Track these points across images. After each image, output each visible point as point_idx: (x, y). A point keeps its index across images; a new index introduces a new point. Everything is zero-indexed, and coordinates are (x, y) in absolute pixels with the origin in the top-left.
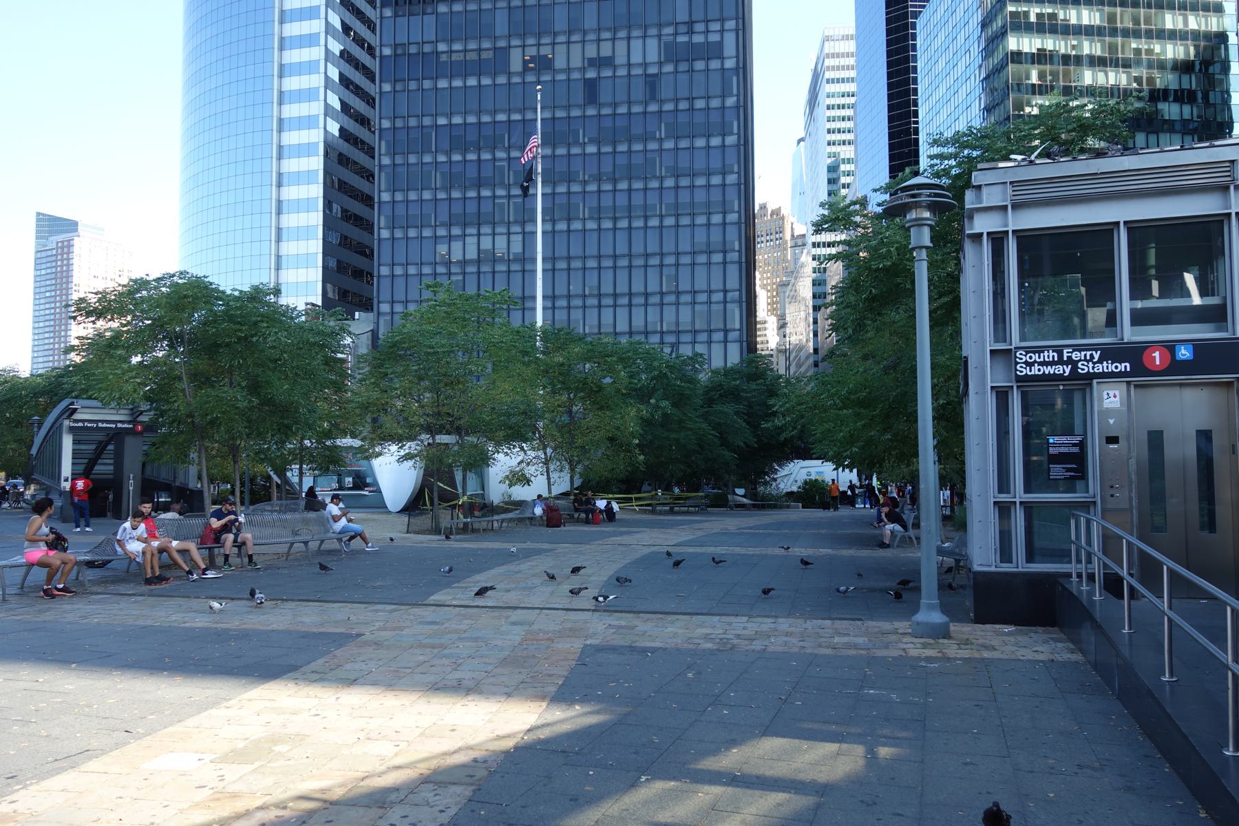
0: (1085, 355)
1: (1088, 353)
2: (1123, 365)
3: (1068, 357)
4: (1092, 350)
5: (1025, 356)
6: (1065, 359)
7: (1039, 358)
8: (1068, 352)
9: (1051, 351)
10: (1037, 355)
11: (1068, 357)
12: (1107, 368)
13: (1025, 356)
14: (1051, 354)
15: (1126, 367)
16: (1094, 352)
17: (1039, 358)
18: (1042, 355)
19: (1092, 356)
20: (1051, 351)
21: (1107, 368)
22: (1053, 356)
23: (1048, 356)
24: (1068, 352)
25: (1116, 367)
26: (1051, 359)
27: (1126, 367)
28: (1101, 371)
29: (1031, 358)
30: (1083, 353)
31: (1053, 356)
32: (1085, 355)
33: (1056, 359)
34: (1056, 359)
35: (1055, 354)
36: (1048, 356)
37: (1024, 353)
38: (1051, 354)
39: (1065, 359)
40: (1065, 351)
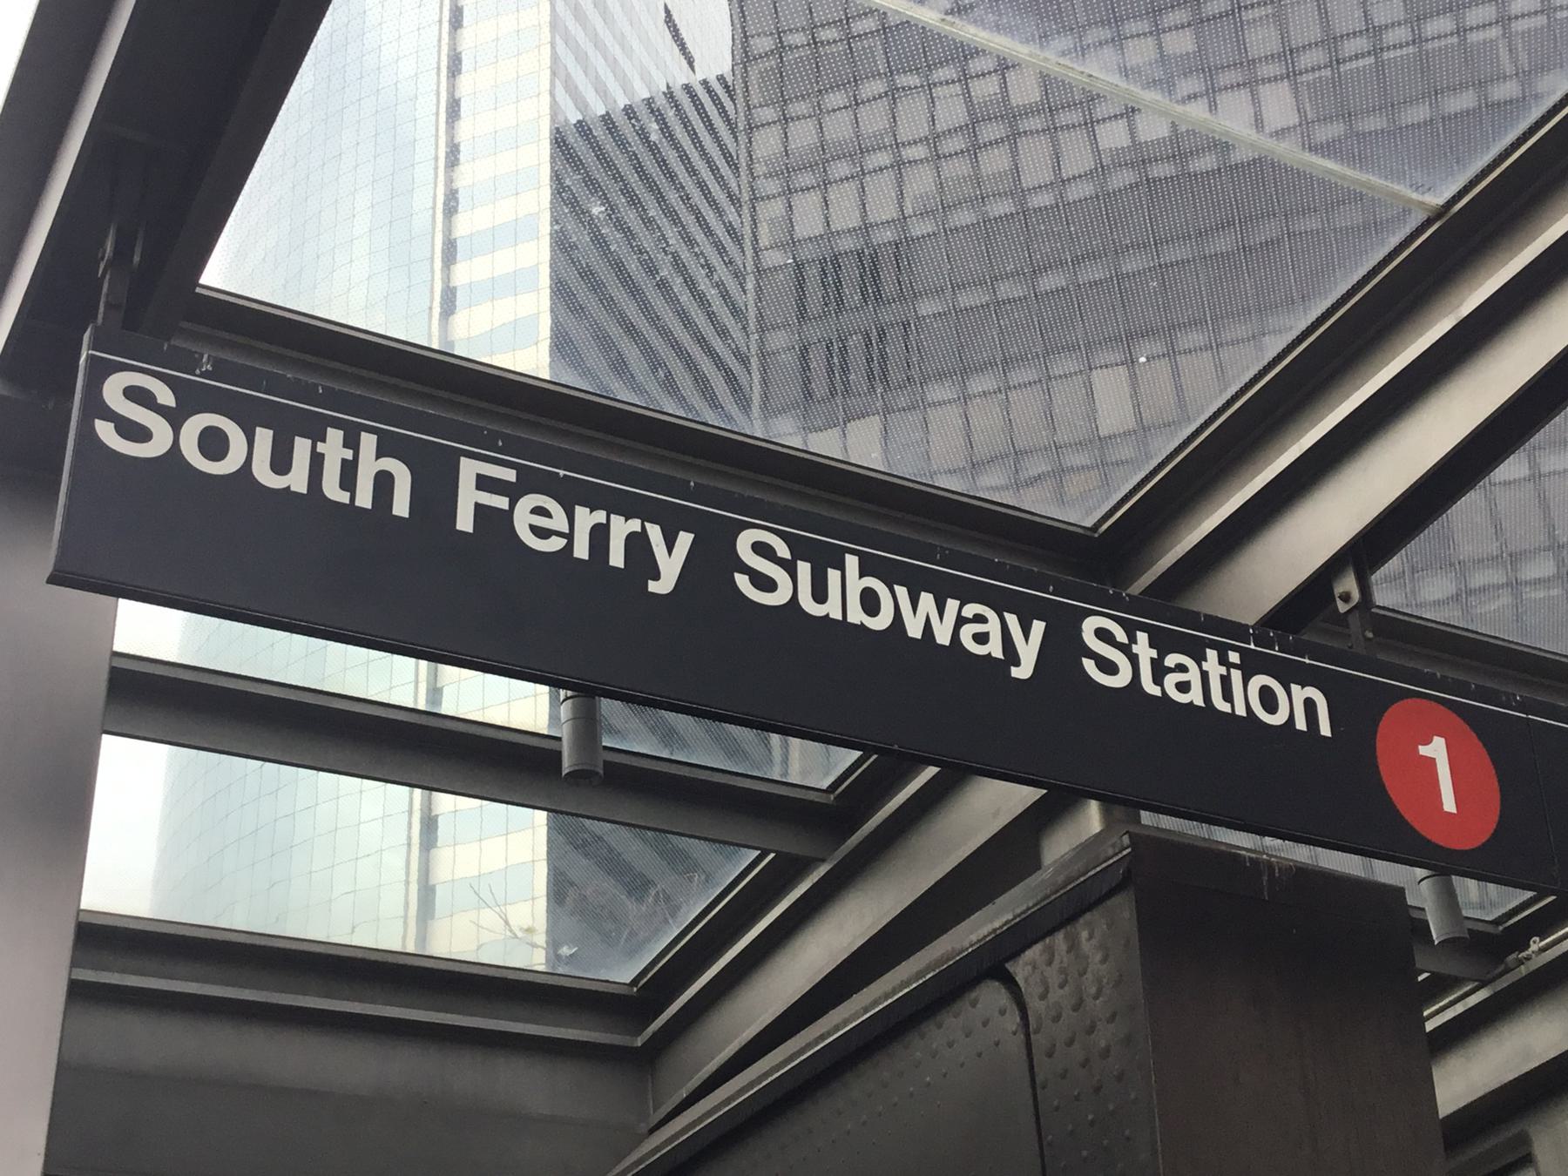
0: (600, 535)
4: (646, 511)
5: (175, 419)
6: (465, 522)
7: (281, 463)
8: (484, 483)
9: (368, 442)
10: (264, 437)
13: (175, 419)
14: (369, 465)
16: (655, 533)
17: (281, 463)
18: (302, 447)
20: (368, 442)
22: (384, 483)
24: (484, 483)
26: (364, 499)
31: (384, 483)
32: (600, 535)
33: (401, 506)
34: (401, 506)
38: (369, 465)
39: (465, 522)
40: (469, 469)
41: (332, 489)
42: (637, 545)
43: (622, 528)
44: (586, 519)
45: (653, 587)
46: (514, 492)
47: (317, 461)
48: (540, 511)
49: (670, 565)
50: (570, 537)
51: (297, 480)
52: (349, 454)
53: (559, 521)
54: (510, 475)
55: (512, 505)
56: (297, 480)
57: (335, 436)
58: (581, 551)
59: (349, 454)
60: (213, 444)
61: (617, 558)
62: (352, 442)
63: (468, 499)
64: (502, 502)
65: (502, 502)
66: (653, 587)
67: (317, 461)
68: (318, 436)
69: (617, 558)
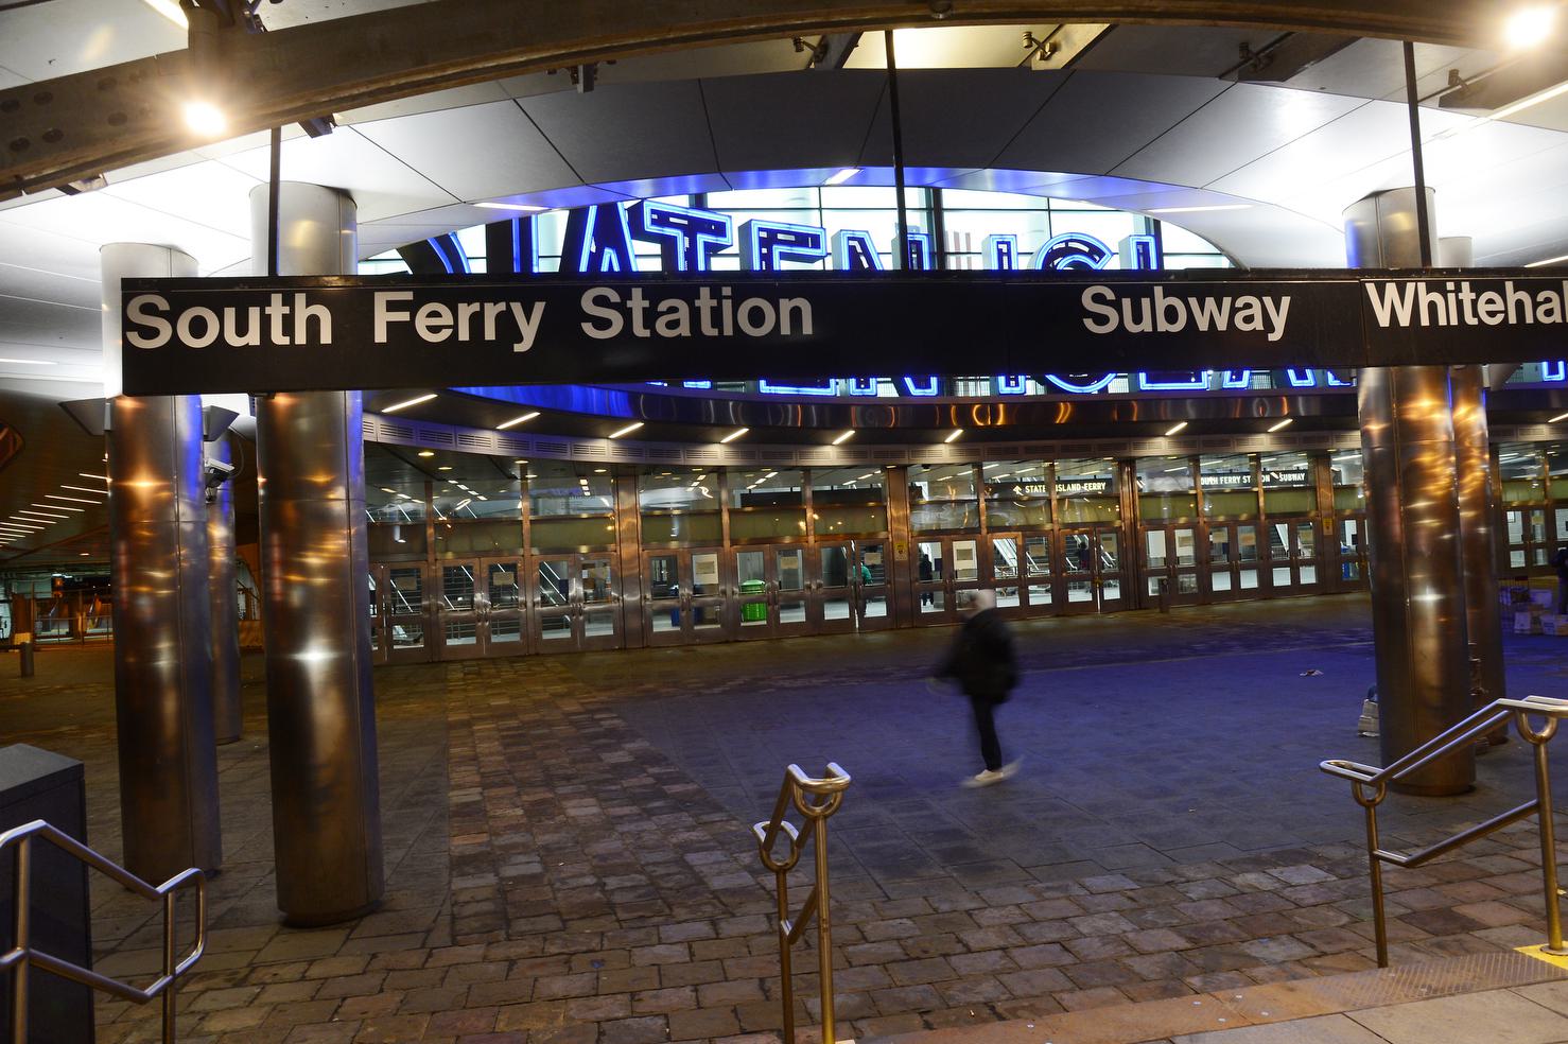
0: (477, 321)
5: (172, 318)
6: (381, 336)
7: (242, 330)
9: (300, 299)
10: (230, 314)
13: (172, 318)
16: (517, 308)
17: (242, 330)
18: (254, 314)
19: (506, 323)
20: (300, 299)
22: (313, 323)
24: (392, 306)
26: (301, 338)
31: (313, 323)
32: (477, 321)
33: (326, 337)
34: (326, 337)
35: (324, 314)
38: (302, 313)
39: (381, 336)
40: (381, 299)
41: (278, 338)
42: (506, 323)
43: (492, 311)
44: (466, 311)
45: (518, 348)
46: (412, 307)
47: (266, 322)
48: (435, 314)
50: (455, 327)
51: (253, 338)
52: (287, 310)
53: (447, 319)
54: (408, 296)
55: (413, 317)
57: (277, 299)
58: (464, 335)
59: (287, 310)
60: (198, 328)
61: (490, 334)
62: (288, 301)
63: (382, 319)
64: (404, 316)
65: (404, 316)
66: (518, 348)
67: (266, 322)
68: (265, 302)
69: (490, 334)
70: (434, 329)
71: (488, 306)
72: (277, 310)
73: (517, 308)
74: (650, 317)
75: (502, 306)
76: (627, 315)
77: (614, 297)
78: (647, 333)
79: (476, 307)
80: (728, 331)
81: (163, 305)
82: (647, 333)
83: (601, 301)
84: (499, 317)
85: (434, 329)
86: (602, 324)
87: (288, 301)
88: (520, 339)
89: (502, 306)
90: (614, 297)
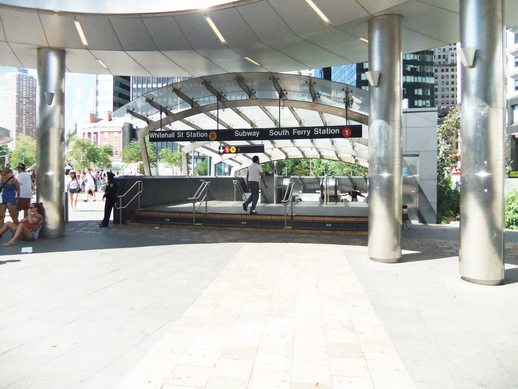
0: (303, 132)
1: (305, 131)
2: (336, 130)
3: (295, 133)
5: (274, 132)
6: (294, 134)
7: (280, 133)
8: (295, 131)
9: (286, 130)
10: (279, 132)
11: (295, 133)
12: (329, 132)
13: (274, 132)
15: (337, 131)
16: (307, 131)
17: (280, 133)
18: (281, 132)
19: (306, 132)
20: (286, 130)
21: (329, 132)
22: (287, 132)
23: (285, 133)
24: (295, 131)
25: (333, 131)
26: (286, 134)
27: (337, 131)
28: (325, 133)
29: (276, 133)
30: (302, 131)
31: (287, 132)
32: (303, 132)
33: (288, 134)
34: (288, 134)
35: (288, 131)
36: (285, 133)
37: (273, 131)
39: (294, 134)
40: (294, 130)
41: (284, 134)
42: (306, 132)
44: (302, 131)
45: (307, 135)
46: (297, 131)
49: (309, 133)
50: (301, 133)
51: (281, 134)
53: (300, 132)
54: (296, 130)
56: (281, 134)
58: (302, 134)
61: (305, 134)
62: (285, 130)
63: (294, 132)
64: (296, 132)
65: (296, 132)
66: (307, 135)
69: (305, 134)
70: (299, 133)
71: (304, 131)
72: (284, 131)
73: (307, 131)
74: (321, 132)
75: (306, 131)
76: (319, 131)
77: (318, 129)
78: (321, 133)
79: (303, 131)
80: (330, 133)
81: (273, 131)
82: (321, 133)
83: (316, 130)
84: (306, 132)
85: (299, 133)
86: (316, 132)
87: (285, 130)
88: (308, 134)
89: (306, 131)
90: (318, 129)
